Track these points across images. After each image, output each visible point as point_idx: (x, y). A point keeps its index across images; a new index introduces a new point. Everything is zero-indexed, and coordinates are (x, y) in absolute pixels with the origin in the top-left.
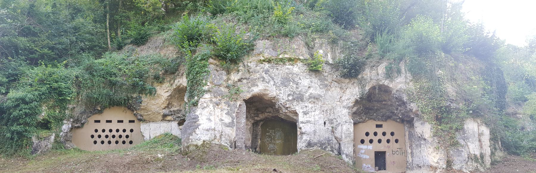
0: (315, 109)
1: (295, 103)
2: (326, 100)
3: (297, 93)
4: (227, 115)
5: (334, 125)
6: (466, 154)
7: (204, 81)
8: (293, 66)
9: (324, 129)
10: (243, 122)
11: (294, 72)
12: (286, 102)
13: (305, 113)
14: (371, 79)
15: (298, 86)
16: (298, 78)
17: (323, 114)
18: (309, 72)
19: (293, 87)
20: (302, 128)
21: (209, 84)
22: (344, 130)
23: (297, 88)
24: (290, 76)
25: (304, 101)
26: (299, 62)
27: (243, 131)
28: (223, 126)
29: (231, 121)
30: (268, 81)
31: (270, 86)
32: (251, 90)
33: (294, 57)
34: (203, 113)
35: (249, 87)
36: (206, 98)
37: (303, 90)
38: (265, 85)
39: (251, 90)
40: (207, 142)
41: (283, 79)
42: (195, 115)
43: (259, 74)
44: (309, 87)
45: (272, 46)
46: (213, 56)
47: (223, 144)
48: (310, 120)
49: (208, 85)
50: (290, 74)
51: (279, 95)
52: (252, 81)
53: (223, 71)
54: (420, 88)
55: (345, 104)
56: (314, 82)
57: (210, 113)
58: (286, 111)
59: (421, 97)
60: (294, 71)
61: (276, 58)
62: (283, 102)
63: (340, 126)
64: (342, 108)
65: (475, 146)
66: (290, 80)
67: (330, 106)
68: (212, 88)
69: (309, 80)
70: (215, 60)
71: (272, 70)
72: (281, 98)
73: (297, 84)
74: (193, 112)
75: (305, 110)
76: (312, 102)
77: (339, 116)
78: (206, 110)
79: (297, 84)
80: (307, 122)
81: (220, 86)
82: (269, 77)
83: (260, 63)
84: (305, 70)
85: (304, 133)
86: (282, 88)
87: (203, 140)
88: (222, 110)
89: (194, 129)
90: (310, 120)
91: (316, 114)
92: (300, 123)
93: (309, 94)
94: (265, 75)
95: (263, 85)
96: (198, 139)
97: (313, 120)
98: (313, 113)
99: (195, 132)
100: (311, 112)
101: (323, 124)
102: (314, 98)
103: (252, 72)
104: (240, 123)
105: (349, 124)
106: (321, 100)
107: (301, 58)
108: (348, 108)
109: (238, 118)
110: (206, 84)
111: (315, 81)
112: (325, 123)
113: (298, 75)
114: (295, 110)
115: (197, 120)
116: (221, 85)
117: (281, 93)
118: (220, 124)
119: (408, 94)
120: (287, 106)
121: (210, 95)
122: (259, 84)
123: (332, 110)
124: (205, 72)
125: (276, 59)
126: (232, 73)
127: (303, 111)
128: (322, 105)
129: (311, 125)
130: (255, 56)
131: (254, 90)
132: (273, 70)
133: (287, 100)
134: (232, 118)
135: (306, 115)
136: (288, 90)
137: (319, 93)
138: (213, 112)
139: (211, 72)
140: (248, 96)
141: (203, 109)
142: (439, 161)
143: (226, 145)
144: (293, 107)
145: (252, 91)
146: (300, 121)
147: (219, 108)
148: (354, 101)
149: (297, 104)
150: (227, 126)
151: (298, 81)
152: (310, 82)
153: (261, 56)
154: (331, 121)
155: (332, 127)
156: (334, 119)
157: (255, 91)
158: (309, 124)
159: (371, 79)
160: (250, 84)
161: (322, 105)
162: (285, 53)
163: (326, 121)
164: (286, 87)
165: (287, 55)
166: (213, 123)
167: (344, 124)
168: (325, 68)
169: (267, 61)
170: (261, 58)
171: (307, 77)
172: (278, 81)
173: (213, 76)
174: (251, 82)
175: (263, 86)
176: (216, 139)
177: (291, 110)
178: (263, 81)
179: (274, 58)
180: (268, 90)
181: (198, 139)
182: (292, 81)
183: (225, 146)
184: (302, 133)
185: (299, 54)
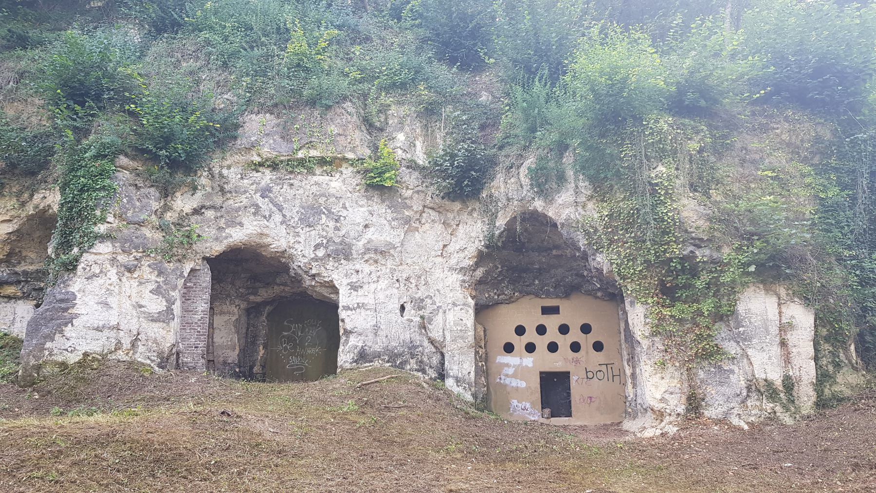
0: (379, 277)
1: (331, 264)
3: (337, 240)
4: (153, 294)
5: (426, 313)
6: (742, 379)
7: (98, 213)
8: (332, 176)
9: (399, 321)
10: (200, 309)
11: (332, 191)
12: (310, 264)
13: (354, 287)
14: (508, 200)
15: (338, 225)
16: (341, 206)
17: (398, 288)
18: (366, 191)
19: (328, 226)
21: (110, 219)
22: (449, 323)
23: (337, 229)
24: (322, 200)
25: (353, 260)
26: (345, 165)
27: (199, 329)
28: (141, 320)
29: (165, 308)
30: (267, 214)
31: (272, 225)
32: (224, 234)
35: (220, 229)
36: (101, 254)
37: (352, 234)
38: (261, 223)
39: (224, 234)
40: (94, 355)
41: (303, 208)
43: (246, 198)
44: (366, 226)
45: (280, 129)
46: (128, 150)
47: (139, 360)
48: (366, 302)
49: (108, 222)
52: (228, 212)
53: (152, 190)
54: (610, 216)
55: (453, 261)
56: (378, 214)
58: (313, 283)
59: (616, 238)
61: (289, 158)
63: (441, 314)
64: (446, 272)
65: (770, 358)
66: (322, 210)
67: (417, 268)
68: (119, 230)
69: (365, 209)
70: (133, 159)
72: (300, 253)
73: (337, 221)
74: (62, 285)
75: (354, 280)
76: (371, 261)
77: (438, 290)
80: (358, 307)
81: (140, 224)
82: (270, 205)
83: (253, 170)
84: (357, 185)
85: (351, 332)
86: (301, 231)
87: (84, 352)
88: (141, 283)
89: (59, 326)
90: (364, 301)
91: (379, 287)
92: (342, 310)
93: (366, 241)
94: (260, 201)
95: (255, 223)
96: (70, 349)
97: (372, 302)
98: (373, 286)
99: (61, 332)
101: (398, 311)
102: (376, 251)
103: (230, 192)
104: (192, 311)
106: (393, 256)
107: (350, 156)
108: (460, 271)
109: (189, 300)
110: (103, 220)
112: (403, 308)
113: (340, 197)
114: (332, 281)
115: (69, 305)
116: (143, 222)
117: (300, 242)
118: (135, 314)
119: (584, 231)
120: (314, 271)
121: (111, 245)
122: (245, 221)
123: (423, 278)
125: (289, 160)
126: (178, 194)
127: (351, 281)
128: (394, 267)
129: (368, 312)
130: (240, 153)
131: (233, 235)
132: (281, 189)
133: (312, 259)
134: (167, 301)
135: (357, 291)
136: (315, 236)
137: (388, 239)
138: (117, 287)
139: (119, 190)
140: (218, 248)
141: (88, 279)
142: (667, 396)
143: (148, 362)
144: (327, 273)
145: (226, 238)
146: (340, 305)
147: (135, 278)
148: (475, 254)
149: (335, 266)
150: (152, 320)
151: (339, 211)
152: (367, 213)
153: (254, 153)
154: (419, 304)
155: (422, 317)
156: (426, 298)
157: (237, 236)
158: (363, 311)
159: (508, 200)
160: (223, 220)
161: (394, 267)
162: (311, 145)
163: (405, 304)
164: (310, 227)
165: (315, 151)
167: (449, 310)
168: (406, 178)
169: (269, 166)
170: (252, 159)
171: (362, 202)
172: (293, 212)
173: (125, 200)
174: (225, 215)
175: (256, 226)
176: (119, 349)
178: (255, 214)
179: (286, 158)
180: (267, 235)
181: (70, 349)
182: (326, 212)
183: (143, 364)
184: (348, 333)
185: (346, 147)
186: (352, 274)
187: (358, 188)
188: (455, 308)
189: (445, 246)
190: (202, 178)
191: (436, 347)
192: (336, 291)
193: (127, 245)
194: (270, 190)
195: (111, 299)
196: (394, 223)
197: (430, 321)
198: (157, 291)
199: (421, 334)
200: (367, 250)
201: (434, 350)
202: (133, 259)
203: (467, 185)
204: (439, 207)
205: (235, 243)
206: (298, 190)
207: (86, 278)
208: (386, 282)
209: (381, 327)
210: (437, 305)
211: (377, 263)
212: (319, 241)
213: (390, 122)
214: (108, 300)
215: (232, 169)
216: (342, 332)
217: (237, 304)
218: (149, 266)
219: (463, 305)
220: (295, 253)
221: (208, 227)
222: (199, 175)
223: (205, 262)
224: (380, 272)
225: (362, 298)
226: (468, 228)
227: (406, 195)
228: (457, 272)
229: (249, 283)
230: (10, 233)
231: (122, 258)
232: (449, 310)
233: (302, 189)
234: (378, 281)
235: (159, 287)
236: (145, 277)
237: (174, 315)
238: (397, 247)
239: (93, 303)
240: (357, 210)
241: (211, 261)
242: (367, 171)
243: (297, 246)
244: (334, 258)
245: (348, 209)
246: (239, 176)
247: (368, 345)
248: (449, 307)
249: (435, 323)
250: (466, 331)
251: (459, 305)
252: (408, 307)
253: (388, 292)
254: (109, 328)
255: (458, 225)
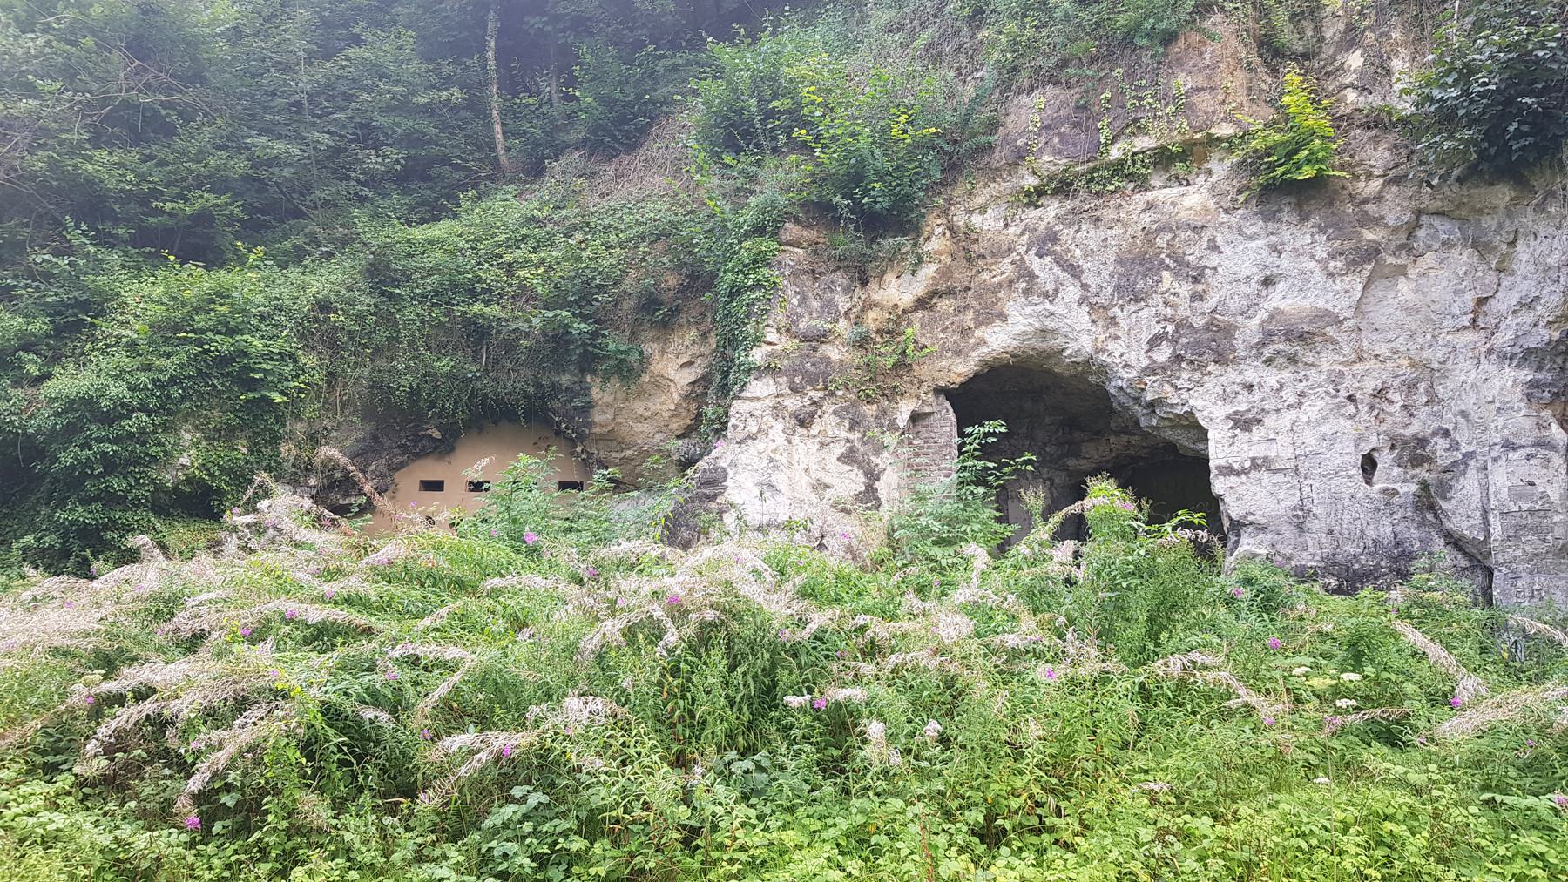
1: (1185, 375)
2: (1375, 335)
3: (1199, 322)
4: (844, 463)
8: (1188, 184)
11: (1184, 216)
13: (1243, 423)
16: (1205, 245)
17: (1352, 417)
20: (1227, 500)
21: (771, 336)
22: (1496, 493)
23: (1198, 297)
24: (1162, 241)
25: (1236, 361)
30: (1050, 288)
33: (1179, 138)
34: (743, 458)
35: (965, 332)
37: (1233, 304)
38: (1040, 308)
39: (972, 341)
44: (1267, 282)
48: (1272, 454)
49: (770, 343)
50: (1163, 229)
51: (1104, 351)
55: (1503, 338)
56: (1295, 250)
58: (1155, 422)
60: (1183, 214)
61: (1092, 165)
62: (1129, 380)
66: (1162, 262)
69: (1260, 243)
70: (808, 227)
71: (1072, 231)
72: (1117, 361)
73: (1196, 280)
75: (1243, 407)
77: (1464, 414)
79: (1195, 278)
80: (1255, 465)
82: (1057, 270)
84: (1240, 192)
86: (1119, 313)
88: (822, 445)
90: (1268, 453)
94: (1035, 263)
95: (1028, 310)
98: (1288, 417)
100: (1278, 411)
101: (1356, 472)
103: (984, 257)
105: (1529, 457)
106: (1334, 342)
107: (1225, 130)
108: (1525, 359)
110: (758, 340)
111: (1297, 244)
113: (1203, 227)
116: (824, 336)
120: (1149, 397)
123: (1422, 386)
126: (890, 277)
127: (1235, 409)
129: (1279, 478)
131: (989, 339)
134: (866, 475)
137: (1321, 304)
138: (785, 455)
140: (960, 370)
141: (740, 443)
146: (1212, 464)
149: (1196, 378)
152: (1265, 253)
153: (1024, 171)
157: (998, 340)
158: (1266, 477)
160: (970, 314)
161: (1338, 368)
163: (1376, 455)
164: (1137, 301)
166: (783, 499)
167: (1495, 460)
171: (1254, 229)
172: (1100, 275)
173: (795, 301)
175: (1031, 315)
177: (1171, 416)
178: (1027, 292)
180: (1053, 331)
182: (1172, 265)
184: (1237, 526)
186: (1237, 393)
187: (1241, 198)
188: (1510, 455)
189: (1481, 301)
190: (933, 239)
191: (1469, 556)
192: (1202, 435)
193: (798, 380)
194: (1052, 237)
196: (1338, 264)
197: (1444, 489)
198: (849, 458)
199: (1422, 524)
200: (1268, 336)
201: (1464, 563)
203: (1519, 134)
204: (1458, 207)
205: (994, 354)
206: (1111, 228)
208: (1321, 404)
209: (1314, 510)
210: (1464, 451)
211: (1296, 362)
212: (1157, 329)
213: (1328, 34)
214: (773, 478)
215: (989, 211)
216: (1226, 523)
217: (1045, 476)
218: (835, 413)
219: (1533, 446)
220: (1109, 360)
221: (943, 331)
222: (926, 235)
223: (942, 398)
224: (1304, 383)
225: (1263, 446)
226: (1540, 247)
227: (1368, 191)
228: (1515, 362)
229: (1060, 434)
230: (694, 383)
232: (1495, 460)
233: (1119, 224)
234: (1300, 404)
235: (851, 450)
236: (830, 433)
237: (878, 499)
238: (1345, 319)
240: (1241, 247)
241: (951, 394)
242: (1258, 155)
243: (1111, 346)
244: (1192, 362)
245: (1222, 249)
246: (1002, 223)
247: (1282, 552)
248: (1494, 454)
249: (1458, 496)
250: (1545, 513)
251: (1523, 447)
252: (1384, 459)
253: (1325, 429)
254: (777, 527)
255: (1512, 244)
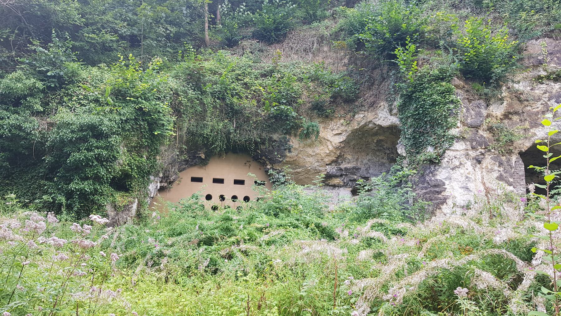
21: (459, 125)
36: (457, 150)
42: (437, 180)
57: (467, 177)
74: (431, 175)
78: (461, 171)
89: (438, 204)
110: (455, 126)
121: (464, 144)
124: (452, 102)
138: (473, 175)
141: (453, 169)
195: (471, 185)
202: (480, 154)
207: (451, 169)
231: (473, 154)
239: (458, 188)
